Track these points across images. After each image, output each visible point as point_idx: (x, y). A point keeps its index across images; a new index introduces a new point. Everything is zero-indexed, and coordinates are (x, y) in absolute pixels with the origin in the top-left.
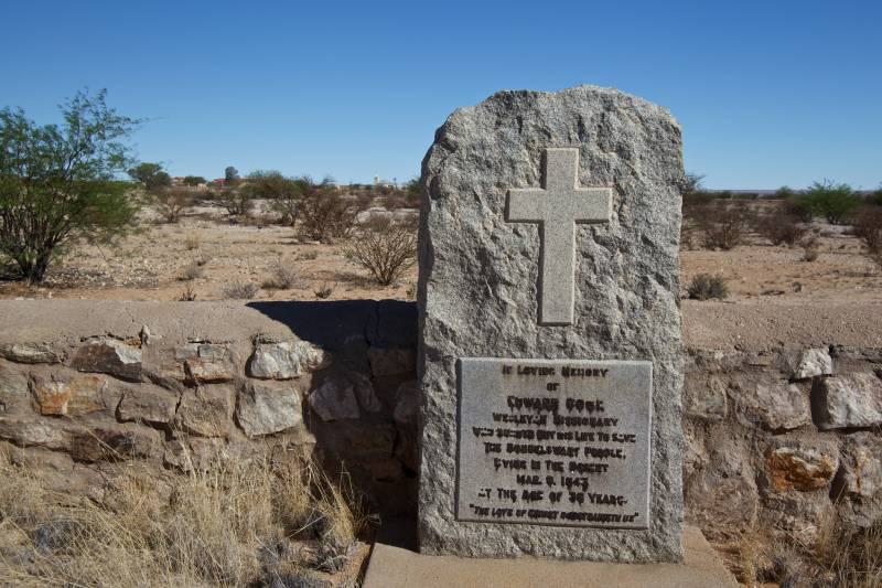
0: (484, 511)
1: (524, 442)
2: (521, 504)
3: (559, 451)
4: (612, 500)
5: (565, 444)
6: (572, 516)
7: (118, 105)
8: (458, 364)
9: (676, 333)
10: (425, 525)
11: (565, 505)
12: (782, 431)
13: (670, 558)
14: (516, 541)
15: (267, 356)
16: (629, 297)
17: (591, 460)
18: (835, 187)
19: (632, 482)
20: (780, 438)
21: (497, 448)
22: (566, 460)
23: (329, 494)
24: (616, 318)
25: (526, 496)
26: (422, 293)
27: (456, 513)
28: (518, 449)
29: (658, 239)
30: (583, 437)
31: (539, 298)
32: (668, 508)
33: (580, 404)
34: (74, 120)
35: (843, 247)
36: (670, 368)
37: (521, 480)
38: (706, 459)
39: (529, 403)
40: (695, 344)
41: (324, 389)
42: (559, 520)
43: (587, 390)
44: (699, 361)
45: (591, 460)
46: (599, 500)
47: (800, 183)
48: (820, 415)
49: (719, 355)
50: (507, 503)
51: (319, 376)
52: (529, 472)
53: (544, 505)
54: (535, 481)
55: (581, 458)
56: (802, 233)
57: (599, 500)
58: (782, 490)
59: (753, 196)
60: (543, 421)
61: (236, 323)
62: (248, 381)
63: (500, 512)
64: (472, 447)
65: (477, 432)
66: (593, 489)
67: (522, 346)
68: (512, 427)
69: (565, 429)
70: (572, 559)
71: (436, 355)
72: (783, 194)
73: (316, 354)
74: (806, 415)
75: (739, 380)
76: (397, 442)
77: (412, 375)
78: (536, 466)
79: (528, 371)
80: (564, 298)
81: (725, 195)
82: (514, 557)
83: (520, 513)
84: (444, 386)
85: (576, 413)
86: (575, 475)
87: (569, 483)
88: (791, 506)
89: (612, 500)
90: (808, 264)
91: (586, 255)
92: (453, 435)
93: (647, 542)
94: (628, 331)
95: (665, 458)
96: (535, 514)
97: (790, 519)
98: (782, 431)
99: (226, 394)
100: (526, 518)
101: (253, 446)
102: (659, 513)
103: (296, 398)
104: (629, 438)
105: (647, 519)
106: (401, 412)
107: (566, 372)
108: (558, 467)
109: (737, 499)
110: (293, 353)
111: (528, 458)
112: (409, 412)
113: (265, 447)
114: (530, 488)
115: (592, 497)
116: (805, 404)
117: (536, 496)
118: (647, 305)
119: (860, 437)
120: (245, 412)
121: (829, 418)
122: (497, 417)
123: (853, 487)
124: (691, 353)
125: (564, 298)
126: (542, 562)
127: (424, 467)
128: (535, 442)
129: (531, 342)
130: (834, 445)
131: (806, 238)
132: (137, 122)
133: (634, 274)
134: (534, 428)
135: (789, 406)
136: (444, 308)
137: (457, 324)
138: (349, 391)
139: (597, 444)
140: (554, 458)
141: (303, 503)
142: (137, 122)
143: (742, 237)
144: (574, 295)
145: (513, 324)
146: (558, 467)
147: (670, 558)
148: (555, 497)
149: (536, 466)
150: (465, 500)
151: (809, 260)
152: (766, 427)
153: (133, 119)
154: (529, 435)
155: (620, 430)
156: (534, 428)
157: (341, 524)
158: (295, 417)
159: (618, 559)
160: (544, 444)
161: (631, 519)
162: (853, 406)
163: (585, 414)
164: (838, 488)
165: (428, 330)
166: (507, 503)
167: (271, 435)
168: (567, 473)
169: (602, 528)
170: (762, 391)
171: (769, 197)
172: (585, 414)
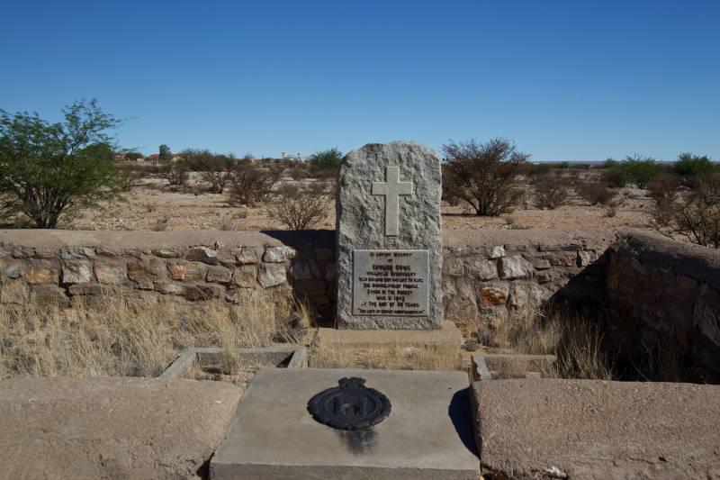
0: (363, 311)
1: (379, 283)
2: (379, 308)
3: (393, 286)
4: (414, 305)
5: (395, 283)
6: (398, 312)
7: (106, 109)
8: (353, 252)
9: (440, 239)
10: (340, 317)
11: (396, 308)
12: (485, 280)
13: (440, 328)
14: (377, 323)
15: (271, 253)
16: (420, 224)
17: (406, 289)
18: (643, 159)
19: (425, 297)
20: (485, 283)
21: (369, 286)
22: (396, 290)
23: (300, 308)
24: (415, 233)
25: (380, 304)
26: (338, 225)
27: (352, 312)
28: (377, 286)
29: (431, 202)
30: (403, 280)
31: (385, 226)
33: (401, 267)
34: (73, 119)
35: (641, 206)
36: (436, 252)
37: (378, 298)
38: (455, 292)
39: (381, 267)
40: (450, 245)
41: (296, 267)
42: (393, 314)
43: (403, 262)
44: (452, 252)
45: (406, 289)
46: (409, 305)
47: (619, 157)
48: (501, 273)
49: (460, 249)
50: (373, 308)
51: (293, 261)
52: (382, 295)
53: (387, 308)
54: (384, 298)
55: (402, 289)
56: (612, 195)
57: (409, 305)
58: (487, 305)
59: (585, 167)
60: (386, 274)
61: (258, 241)
62: (262, 264)
63: (370, 311)
64: (359, 286)
65: (360, 279)
66: (406, 301)
67: (378, 245)
68: (374, 277)
69: (395, 277)
70: (399, 329)
71: (344, 249)
72: (609, 164)
73: (292, 251)
74: (495, 273)
75: (468, 260)
76: (327, 288)
77: (334, 259)
78: (384, 292)
79: (381, 254)
80: (395, 225)
81: (564, 166)
82: (375, 329)
83: (378, 311)
84: (347, 261)
85: (400, 271)
86: (400, 295)
87: (397, 299)
88: (490, 311)
89: (414, 305)
90: (608, 220)
91: (403, 208)
92: (351, 281)
94: (419, 238)
95: (434, 288)
96: (384, 312)
98: (485, 280)
99: (254, 269)
100: (380, 313)
101: (265, 292)
102: (432, 310)
103: (284, 271)
104: (420, 280)
106: (329, 276)
107: (396, 255)
108: (393, 292)
109: (469, 309)
110: (282, 252)
111: (381, 289)
112: (332, 275)
113: (272, 291)
114: (382, 301)
116: (495, 269)
117: (384, 304)
118: (427, 228)
119: (517, 282)
120: (262, 277)
121: (504, 274)
122: (368, 273)
123: (514, 303)
124: (449, 249)
125: (395, 225)
127: (339, 294)
128: (383, 283)
129: (382, 243)
130: (506, 285)
131: (616, 199)
132: (118, 121)
133: (422, 216)
134: (383, 277)
135: (488, 270)
136: (347, 230)
137: (352, 236)
138: (307, 267)
139: (408, 283)
140: (391, 289)
142: (118, 121)
143: (567, 199)
144: (398, 224)
145: (375, 236)
146: (393, 292)
147: (440, 328)
148: (392, 305)
149: (384, 292)
151: (610, 216)
152: (479, 278)
153: (116, 119)
154: (381, 280)
155: (417, 277)
156: (383, 277)
157: (305, 320)
158: (284, 279)
159: (416, 329)
160: (387, 283)
161: (421, 312)
162: (513, 269)
163: (403, 271)
164: (510, 306)
165: (340, 239)
166: (373, 308)
167: (275, 286)
168: (396, 295)
169: (410, 316)
170: (477, 264)
171: (598, 167)
172: (403, 271)
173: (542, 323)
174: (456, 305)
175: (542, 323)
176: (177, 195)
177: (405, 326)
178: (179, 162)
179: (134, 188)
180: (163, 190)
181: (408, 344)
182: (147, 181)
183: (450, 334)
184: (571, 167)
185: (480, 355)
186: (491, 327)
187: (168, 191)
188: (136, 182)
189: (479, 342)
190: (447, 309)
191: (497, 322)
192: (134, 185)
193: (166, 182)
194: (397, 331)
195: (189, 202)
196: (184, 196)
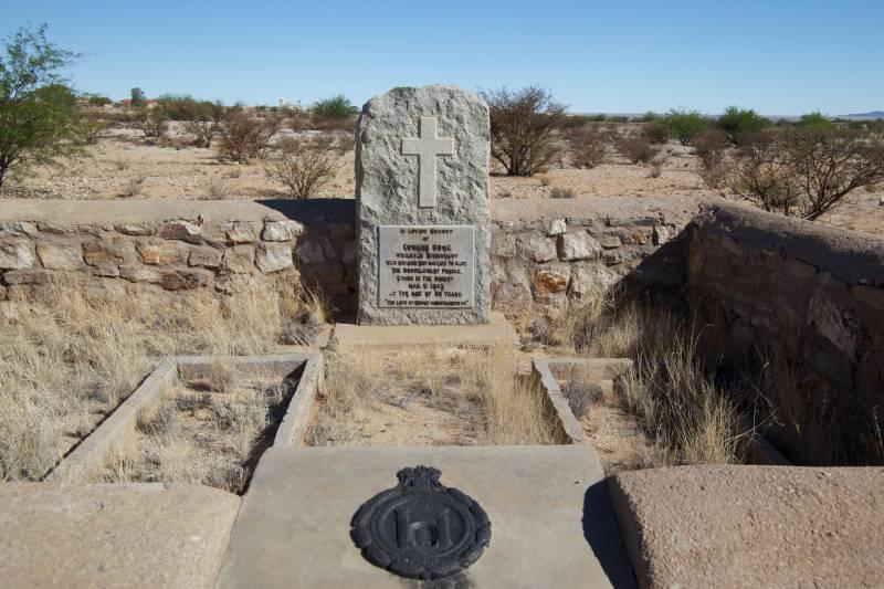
0: (393, 303)
1: (412, 267)
2: (411, 298)
3: (429, 271)
4: (456, 295)
5: (432, 267)
6: (436, 303)
7: (57, 40)
8: (378, 229)
9: (488, 212)
10: (362, 311)
11: (433, 298)
12: (542, 262)
13: (483, 322)
14: (409, 316)
15: (272, 229)
16: (463, 193)
17: (445, 275)
18: (687, 112)
19: (465, 285)
20: (542, 266)
21: (398, 271)
22: (433, 276)
23: (312, 298)
24: (457, 204)
25: (413, 294)
26: (358, 193)
28: (409, 271)
29: (477, 164)
30: (441, 264)
31: (418, 194)
32: (483, 297)
33: (439, 248)
34: (16, 53)
35: (686, 165)
36: (483, 229)
37: (411, 286)
38: (505, 278)
39: (414, 248)
40: (499, 219)
41: (305, 246)
42: (430, 306)
43: (442, 240)
44: (501, 227)
45: (445, 275)
46: (448, 294)
47: (662, 108)
48: (561, 254)
49: (511, 224)
50: (404, 298)
51: (301, 240)
52: (415, 282)
53: (422, 298)
54: (418, 287)
55: (440, 274)
56: (655, 152)
57: (448, 294)
58: (543, 292)
59: (623, 120)
60: (421, 256)
61: (254, 213)
62: (261, 243)
63: (400, 303)
64: (386, 271)
65: (388, 263)
66: (445, 290)
67: (410, 219)
68: (406, 260)
69: (432, 260)
71: (366, 224)
72: (649, 118)
73: (299, 227)
74: (554, 254)
75: (522, 237)
76: (345, 273)
77: (354, 237)
78: (418, 279)
79: (413, 231)
80: (431, 194)
81: (600, 118)
83: (411, 303)
84: (371, 240)
85: (437, 252)
86: (437, 283)
87: (434, 287)
88: (547, 299)
89: (456, 295)
90: (652, 180)
91: (441, 172)
92: (376, 264)
93: (473, 314)
94: (462, 210)
95: (481, 273)
96: (418, 303)
97: (547, 307)
98: (542, 262)
99: (250, 250)
100: (413, 305)
101: (266, 278)
102: (478, 300)
103: (289, 252)
104: (463, 264)
105: (473, 303)
106: (347, 258)
107: (432, 231)
108: (429, 279)
109: (521, 297)
110: (286, 228)
111: (414, 275)
112: (350, 258)
113: (273, 278)
114: (415, 290)
115: (446, 294)
116: (554, 248)
117: (418, 294)
118: (472, 197)
119: (579, 264)
120: (261, 259)
121: (565, 255)
122: (398, 255)
123: (576, 290)
124: (498, 223)
125: (431, 194)
126: (422, 327)
127: (361, 282)
128: (417, 267)
129: (414, 217)
130: (567, 268)
131: (658, 158)
132: (79, 55)
133: (465, 182)
134: (417, 260)
135: (546, 249)
136: (370, 200)
137: (376, 208)
138: (318, 247)
139: (447, 267)
140: (426, 275)
141: (295, 307)
142: (79, 55)
143: (606, 157)
144: (436, 193)
145: (405, 208)
146: (429, 279)
147: (483, 322)
148: (427, 294)
149: (418, 279)
150: (382, 297)
151: (654, 177)
152: (535, 261)
153: (75, 53)
154: (414, 263)
155: (459, 260)
156: (417, 260)
157: (318, 315)
158: (289, 262)
159: (459, 323)
160: (422, 268)
161: (465, 303)
162: (576, 248)
163: (442, 252)
164: (570, 290)
165: (362, 212)
166: (404, 298)
167: (277, 272)
168: (433, 282)
169: (451, 309)
170: (533, 242)
171: (637, 120)
172: (442, 252)
173: (613, 314)
174: (505, 292)
175: (613, 314)
176: (154, 149)
177: (444, 321)
178: (156, 109)
179: (101, 141)
180: (136, 142)
181: (450, 345)
182: (116, 132)
183: (500, 331)
184: (610, 120)
185: (541, 358)
186: (549, 319)
187: (143, 144)
188: (103, 132)
189: (537, 339)
190: (494, 297)
191: (555, 313)
192: (101, 137)
193: (141, 133)
194: (434, 328)
195: (169, 159)
196: (163, 150)
